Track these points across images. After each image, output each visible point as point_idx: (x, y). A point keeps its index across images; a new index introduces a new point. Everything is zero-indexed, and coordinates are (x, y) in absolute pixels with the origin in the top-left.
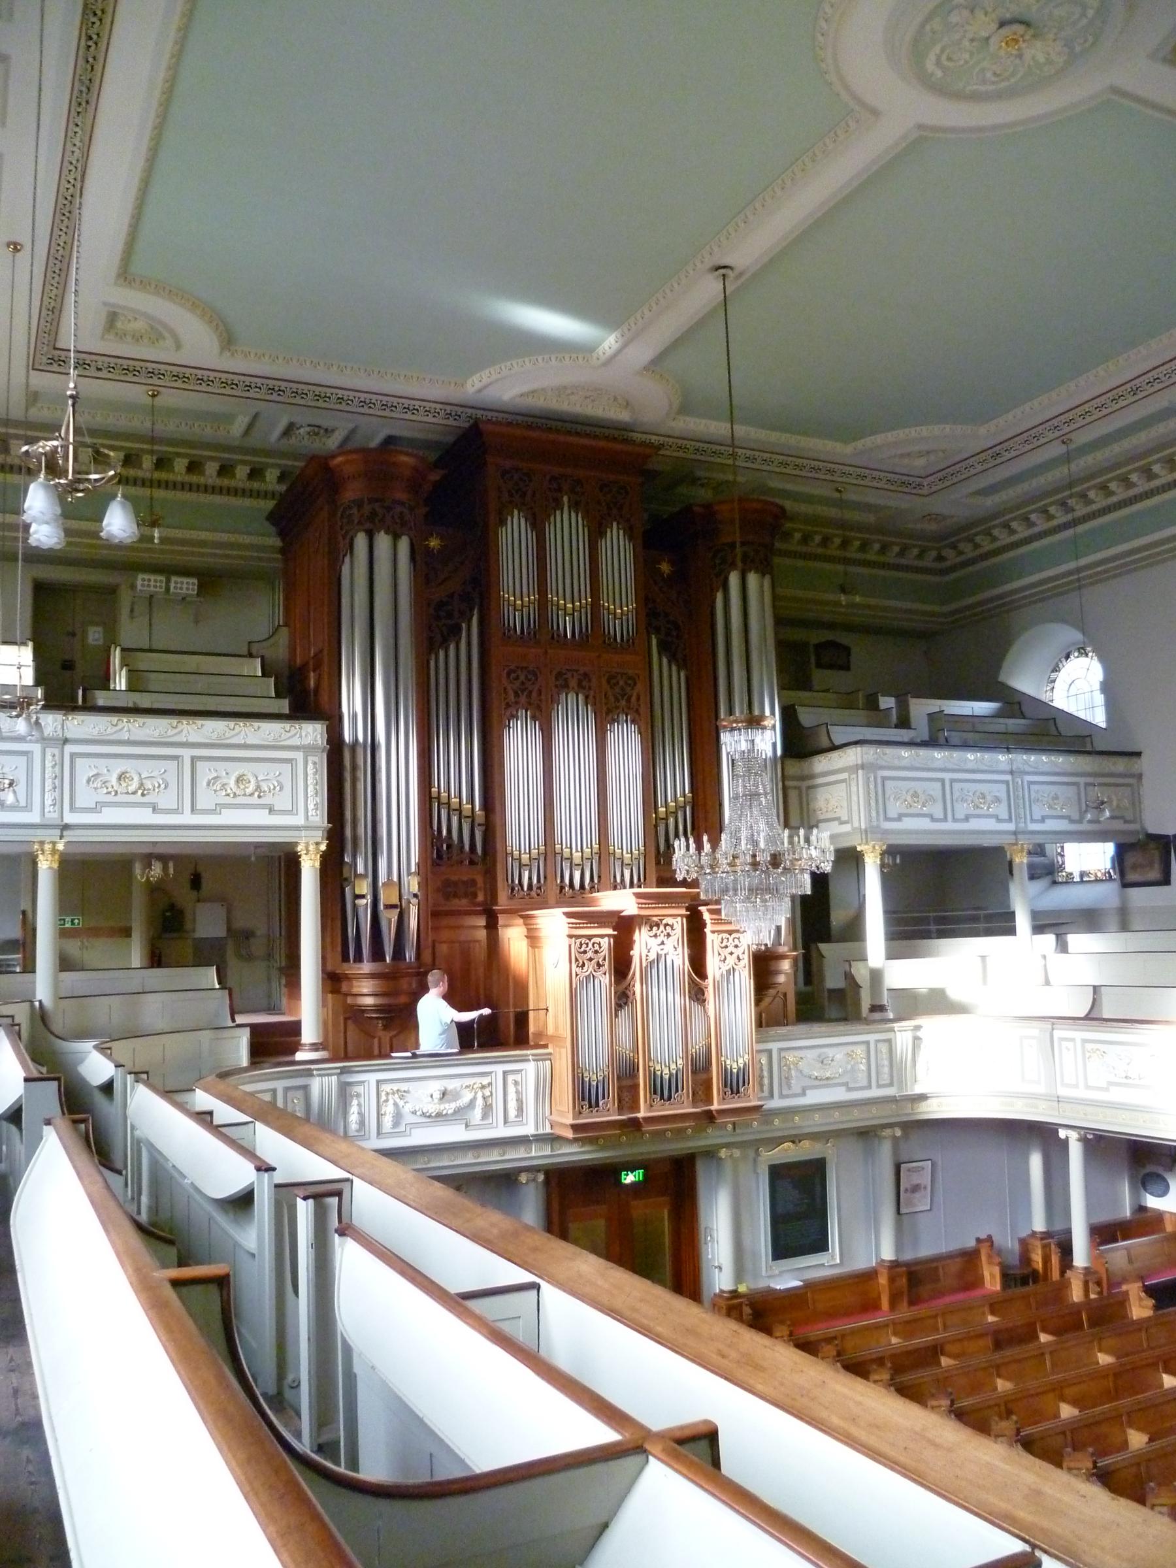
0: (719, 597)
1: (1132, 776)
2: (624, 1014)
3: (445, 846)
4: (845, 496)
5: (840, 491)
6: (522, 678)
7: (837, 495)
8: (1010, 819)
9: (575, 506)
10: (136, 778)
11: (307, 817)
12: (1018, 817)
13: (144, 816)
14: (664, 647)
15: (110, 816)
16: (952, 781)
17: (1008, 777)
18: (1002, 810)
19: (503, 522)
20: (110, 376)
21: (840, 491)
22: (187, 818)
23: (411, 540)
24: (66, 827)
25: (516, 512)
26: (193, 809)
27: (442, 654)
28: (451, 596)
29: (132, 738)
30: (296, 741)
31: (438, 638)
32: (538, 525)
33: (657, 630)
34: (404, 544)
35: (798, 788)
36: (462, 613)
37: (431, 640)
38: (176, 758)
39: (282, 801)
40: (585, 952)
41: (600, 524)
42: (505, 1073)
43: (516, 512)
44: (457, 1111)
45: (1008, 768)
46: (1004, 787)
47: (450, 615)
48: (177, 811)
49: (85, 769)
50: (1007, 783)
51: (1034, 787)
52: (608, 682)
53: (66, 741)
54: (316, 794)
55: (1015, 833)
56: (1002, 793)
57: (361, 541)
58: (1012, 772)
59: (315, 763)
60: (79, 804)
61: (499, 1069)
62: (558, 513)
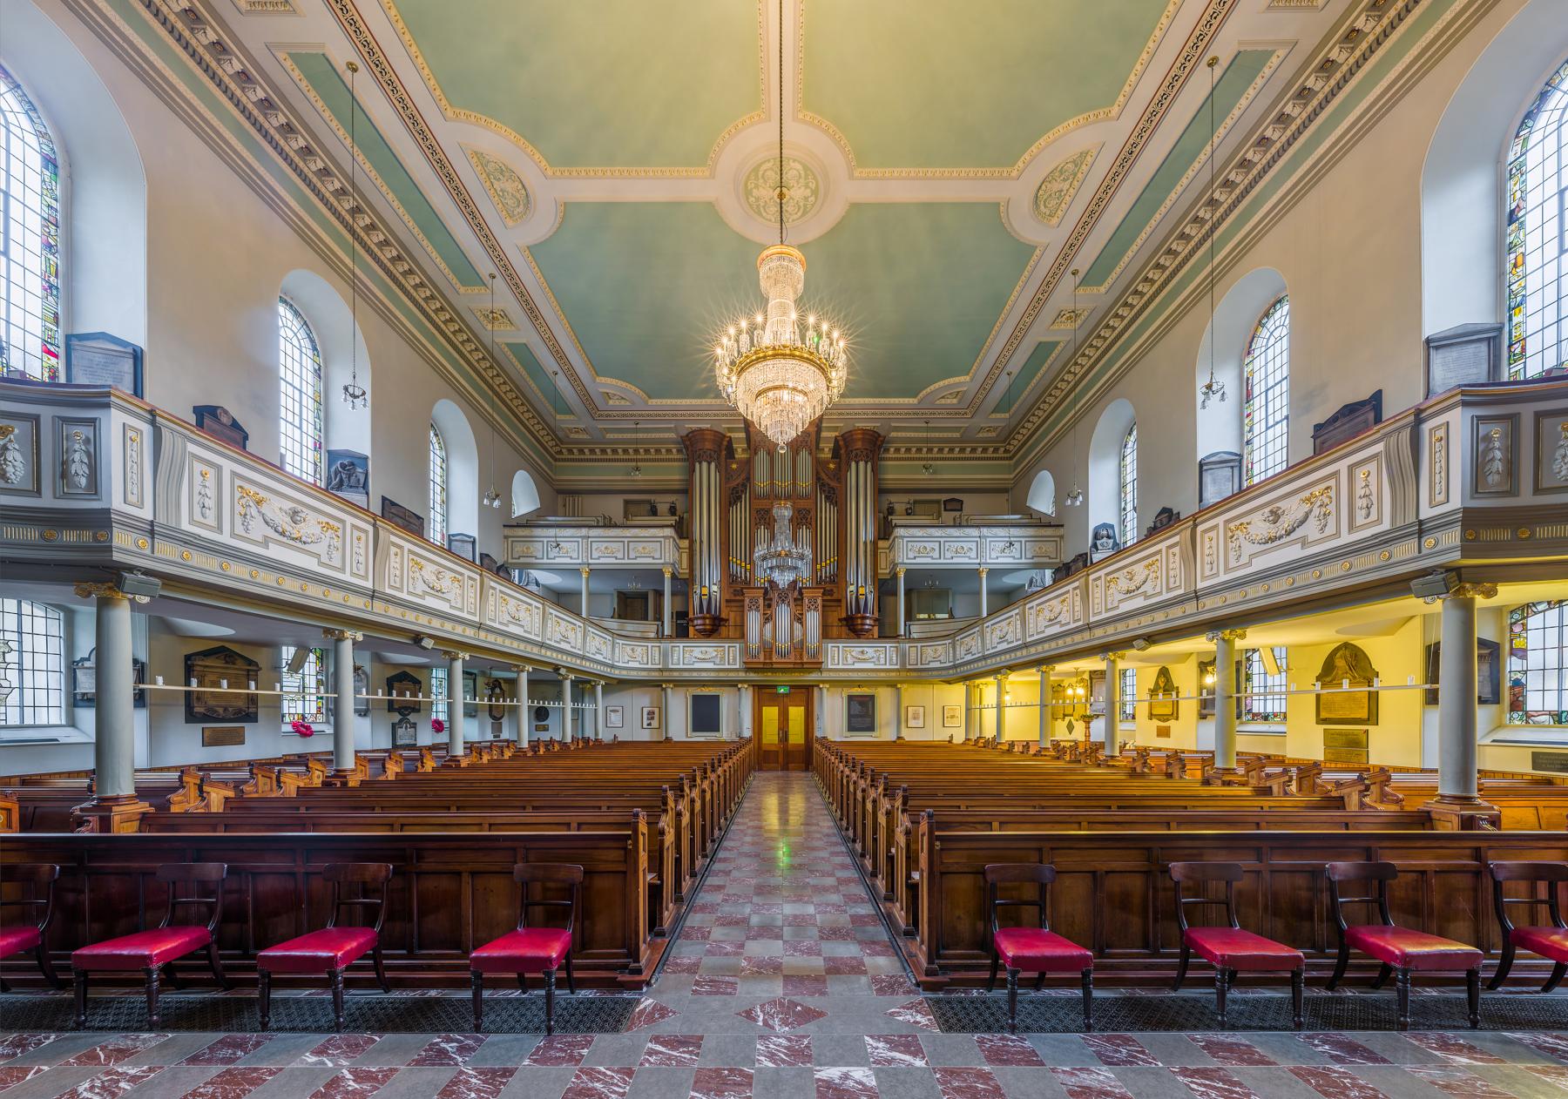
2: (769, 626)
13: (613, 561)
14: (827, 498)
15: (602, 561)
22: (626, 561)
24: (589, 564)
39: (657, 555)
47: (737, 492)
57: (697, 465)
61: (727, 645)
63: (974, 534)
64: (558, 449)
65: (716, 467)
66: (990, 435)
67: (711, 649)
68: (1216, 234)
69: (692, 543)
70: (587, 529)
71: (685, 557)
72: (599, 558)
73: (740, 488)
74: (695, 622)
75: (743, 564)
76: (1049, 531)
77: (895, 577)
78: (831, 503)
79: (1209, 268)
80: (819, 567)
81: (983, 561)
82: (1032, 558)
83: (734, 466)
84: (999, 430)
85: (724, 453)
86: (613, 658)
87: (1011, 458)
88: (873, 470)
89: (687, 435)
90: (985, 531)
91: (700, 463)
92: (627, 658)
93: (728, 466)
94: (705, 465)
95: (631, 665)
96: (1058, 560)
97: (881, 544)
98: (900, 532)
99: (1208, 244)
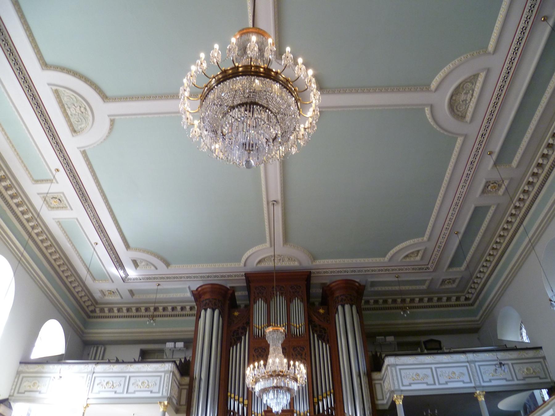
0: (337, 315)
1: (540, 358)
3: (232, 413)
4: (400, 279)
5: (398, 277)
6: (260, 351)
7: (396, 279)
8: (471, 382)
9: (281, 294)
10: (112, 383)
12: (474, 380)
14: (319, 337)
16: (436, 368)
17: (467, 364)
18: (467, 379)
19: (255, 302)
21: (398, 277)
23: (219, 311)
25: (260, 299)
26: (127, 392)
27: (235, 347)
28: (239, 328)
30: (163, 369)
31: (233, 341)
32: (267, 302)
33: (316, 331)
34: (216, 312)
35: (381, 384)
36: (242, 333)
37: (231, 343)
38: (125, 377)
41: (290, 299)
43: (260, 299)
45: (466, 360)
46: (465, 368)
47: (238, 334)
48: (123, 393)
49: (97, 381)
50: (467, 366)
51: (481, 367)
52: (293, 350)
53: (94, 373)
55: (475, 387)
56: (464, 370)
57: (203, 312)
58: (468, 362)
59: (167, 376)
63: (462, 360)
64: (92, 308)
65: (220, 313)
66: (450, 286)
68: (525, 223)
69: (192, 380)
70: (94, 366)
71: (184, 393)
72: (99, 392)
73: (240, 331)
75: (241, 400)
76: (531, 354)
77: (393, 404)
78: (323, 340)
79: (527, 240)
80: (316, 400)
81: (478, 384)
82: (524, 379)
83: (236, 314)
84: (457, 281)
85: (228, 302)
87: (472, 305)
88: (358, 312)
89: (197, 289)
90: (471, 356)
91: (206, 310)
93: (230, 315)
94: (209, 311)
96: (549, 380)
97: (375, 375)
98: (389, 361)
99: (522, 228)
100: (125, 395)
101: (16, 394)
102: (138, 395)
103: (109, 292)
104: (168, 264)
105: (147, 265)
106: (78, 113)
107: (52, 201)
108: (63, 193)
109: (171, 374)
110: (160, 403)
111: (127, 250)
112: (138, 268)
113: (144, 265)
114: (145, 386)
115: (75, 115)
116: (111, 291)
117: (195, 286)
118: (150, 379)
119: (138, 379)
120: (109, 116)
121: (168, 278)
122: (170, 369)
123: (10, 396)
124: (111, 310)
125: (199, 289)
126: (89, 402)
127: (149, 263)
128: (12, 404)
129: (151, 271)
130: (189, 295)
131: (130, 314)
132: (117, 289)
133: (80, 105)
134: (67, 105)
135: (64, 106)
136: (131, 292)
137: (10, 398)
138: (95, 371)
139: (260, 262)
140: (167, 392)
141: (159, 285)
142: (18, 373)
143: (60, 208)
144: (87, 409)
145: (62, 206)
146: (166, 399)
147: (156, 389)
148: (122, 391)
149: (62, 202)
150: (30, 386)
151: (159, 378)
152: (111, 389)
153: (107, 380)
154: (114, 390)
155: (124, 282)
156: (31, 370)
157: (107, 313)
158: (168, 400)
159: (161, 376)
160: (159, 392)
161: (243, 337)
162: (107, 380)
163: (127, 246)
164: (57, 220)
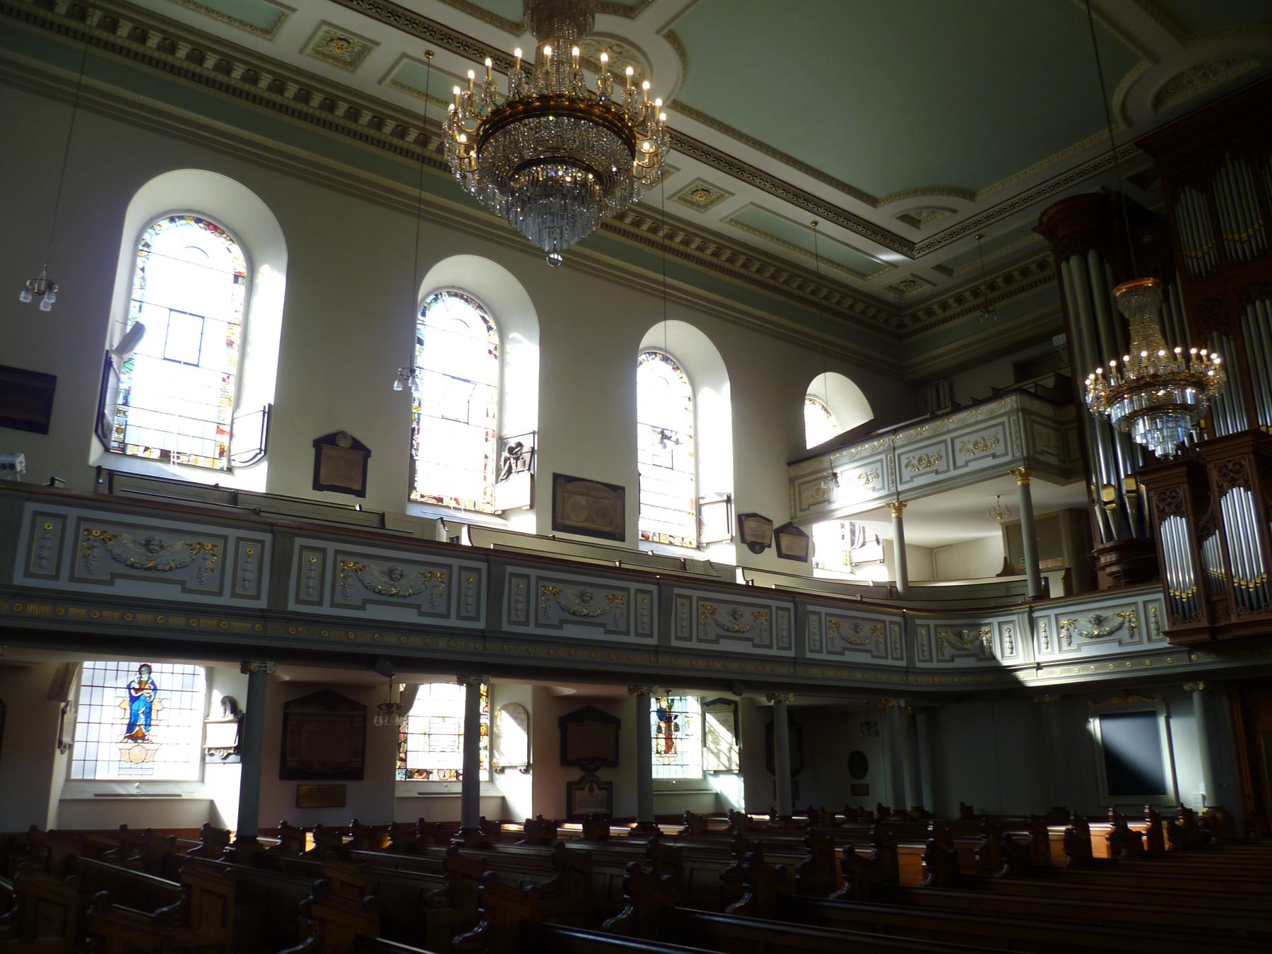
2: (1212, 544)
11: (1013, 454)
20: (947, 242)
24: (898, 493)
26: (955, 468)
29: (923, 437)
30: (1003, 411)
38: (945, 441)
40: (1164, 500)
42: (1145, 603)
44: (1110, 633)
48: (948, 470)
53: (894, 449)
54: (1017, 438)
57: (1064, 265)
59: (1014, 420)
60: (904, 479)
61: (1140, 600)
62: (1223, 170)
67: (1108, 613)
74: (1103, 560)
86: (910, 658)
91: (1067, 260)
92: (948, 651)
94: (1074, 261)
95: (960, 663)
100: (953, 473)
101: (799, 514)
102: (973, 466)
103: (904, 284)
104: (970, 195)
105: (933, 212)
106: (617, 57)
107: (697, 198)
108: (699, 179)
109: (1020, 414)
110: (1013, 472)
111: (876, 208)
112: (922, 226)
113: (928, 216)
114: (981, 449)
115: (615, 62)
116: (906, 281)
117: (1032, 216)
118: (986, 434)
119: (965, 439)
120: (658, 32)
121: (1000, 212)
122: (1015, 406)
123: (792, 518)
124: (930, 312)
125: (1045, 218)
126: (902, 498)
127: (934, 210)
128: (802, 528)
129: (945, 221)
130: (1037, 237)
131: (966, 306)
132: (912, 275)
133: (608, 45)
134: (591, 56)
135: (590, 61)
136: (940, 268)
137: (794, 521)
138: (896, 445)
139: (1158, 100)
140: (1020, 449)
141: (981, 237)
142: (792, 480)
143: (716, 200)
144: (905, 510)
145: (716, 197)
146: (1022, 463)
147: (999, 449)
148: (946, 469)
149: (711, 191)
150: (813, 496)
151: (1001, 427)
152: (928, 469)
153: (917, 454)
154: (933, 468)
155: (914, 259)
156: (808, 471)
157: (940, 314)
158: (1026, 462)
159: (1002, 424)
160: (1006, 454)
161: (1170, 287)
162: (917, 454)
163: (872, 201)
164: (727, 220)
